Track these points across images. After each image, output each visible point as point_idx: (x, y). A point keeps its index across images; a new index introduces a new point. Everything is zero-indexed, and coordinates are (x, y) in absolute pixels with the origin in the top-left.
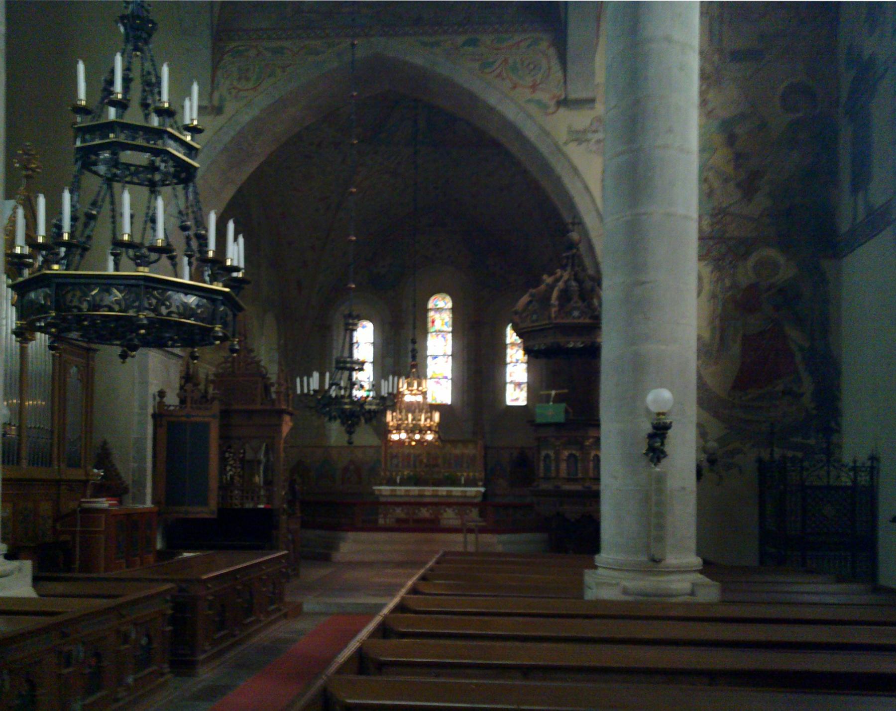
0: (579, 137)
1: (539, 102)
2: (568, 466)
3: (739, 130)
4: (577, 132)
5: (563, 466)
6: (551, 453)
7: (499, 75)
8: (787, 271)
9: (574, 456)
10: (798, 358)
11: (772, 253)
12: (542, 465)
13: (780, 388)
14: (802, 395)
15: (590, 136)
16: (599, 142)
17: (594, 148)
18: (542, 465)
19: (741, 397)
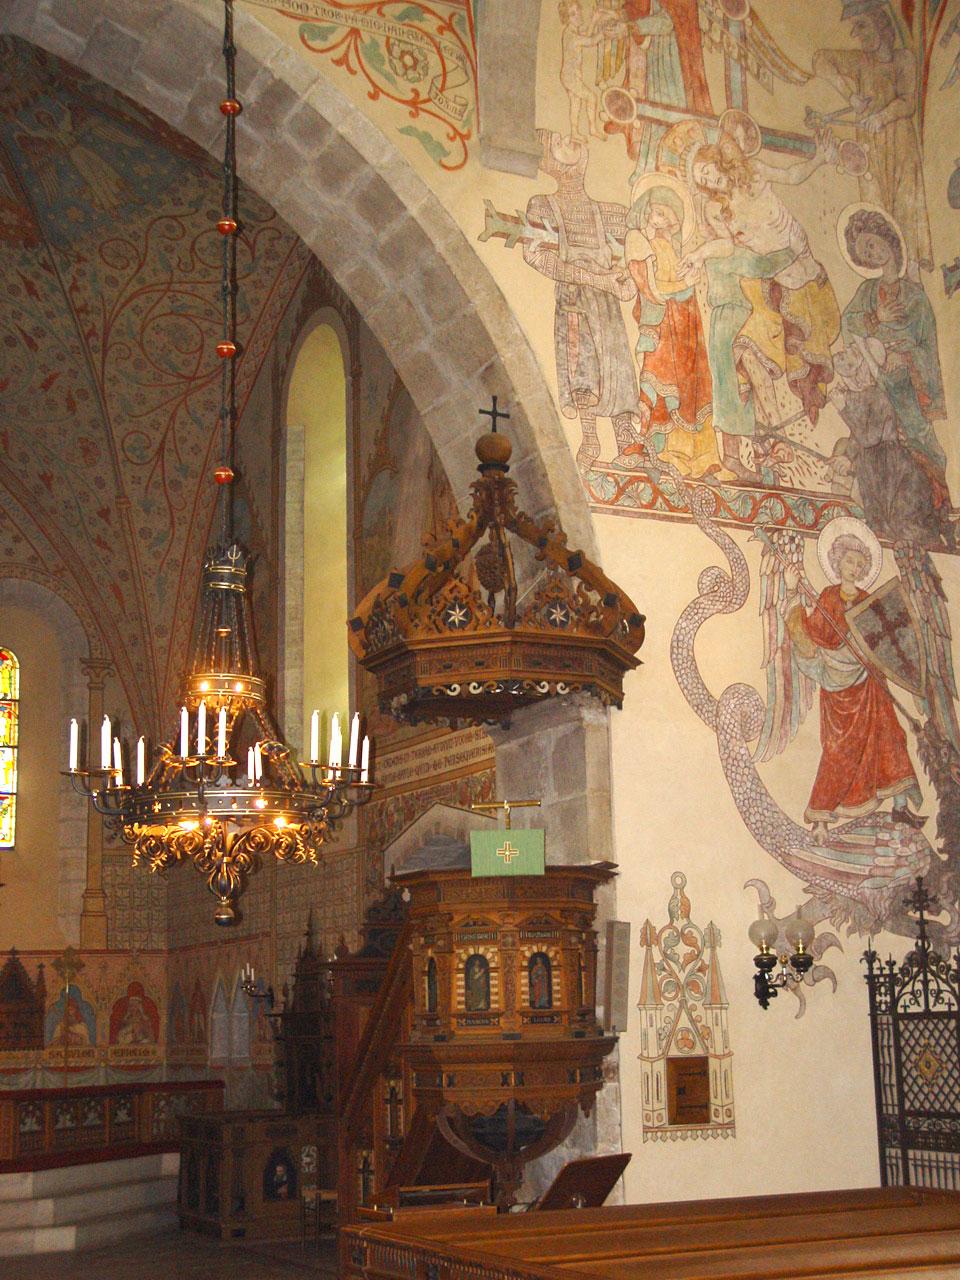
0: (508, 228)
1: (425, 138)
2: (531, 985)
3: (784, 280)
4: (504, 217)
5: (523, 980)
6: (491, 953)
7: (342, 62)
8: (883, 570)
9: (543, 956)
10: (912, 743)
11: (856, 529)
12: (459, 981)
13: (888, 806)
14: (922, 822)
15: (528, 231)
16: (545, 247)
17: (538, 259)
18: (459, 981)
19: (825, 823)
